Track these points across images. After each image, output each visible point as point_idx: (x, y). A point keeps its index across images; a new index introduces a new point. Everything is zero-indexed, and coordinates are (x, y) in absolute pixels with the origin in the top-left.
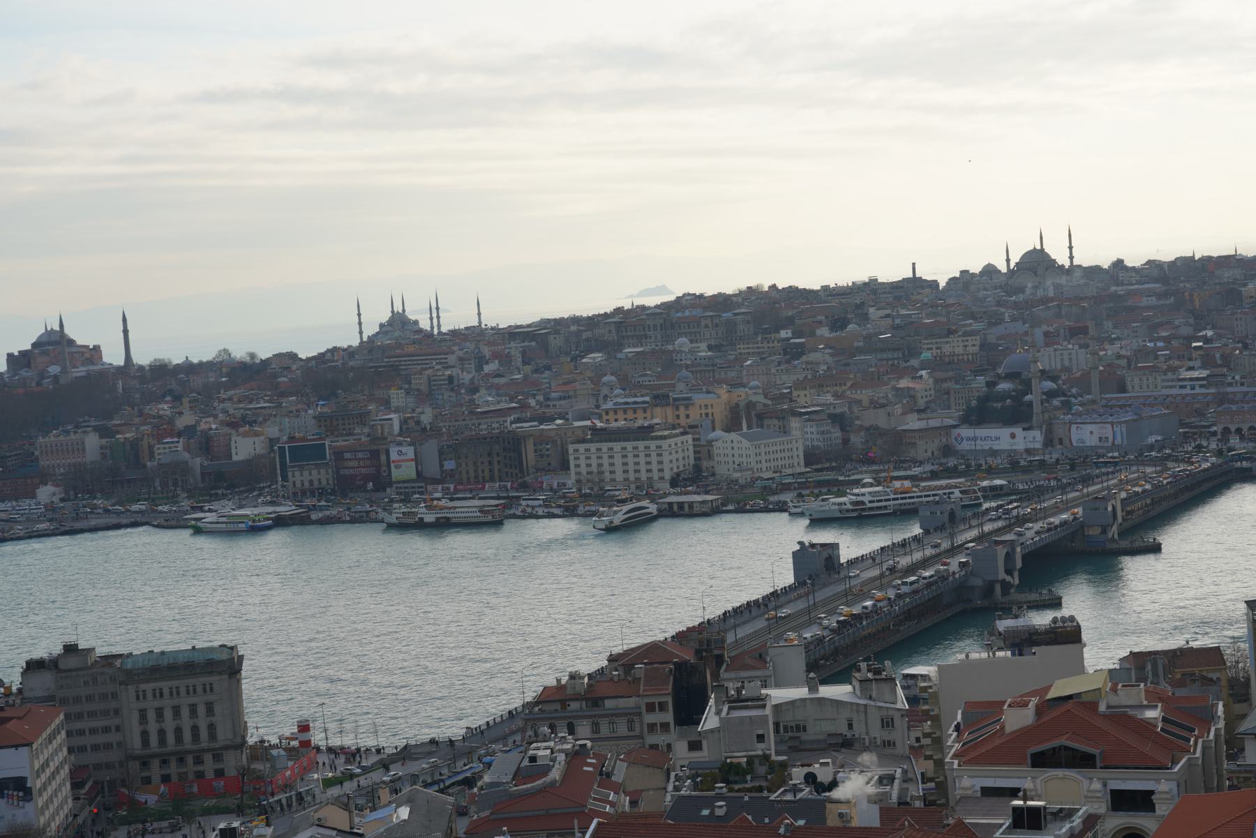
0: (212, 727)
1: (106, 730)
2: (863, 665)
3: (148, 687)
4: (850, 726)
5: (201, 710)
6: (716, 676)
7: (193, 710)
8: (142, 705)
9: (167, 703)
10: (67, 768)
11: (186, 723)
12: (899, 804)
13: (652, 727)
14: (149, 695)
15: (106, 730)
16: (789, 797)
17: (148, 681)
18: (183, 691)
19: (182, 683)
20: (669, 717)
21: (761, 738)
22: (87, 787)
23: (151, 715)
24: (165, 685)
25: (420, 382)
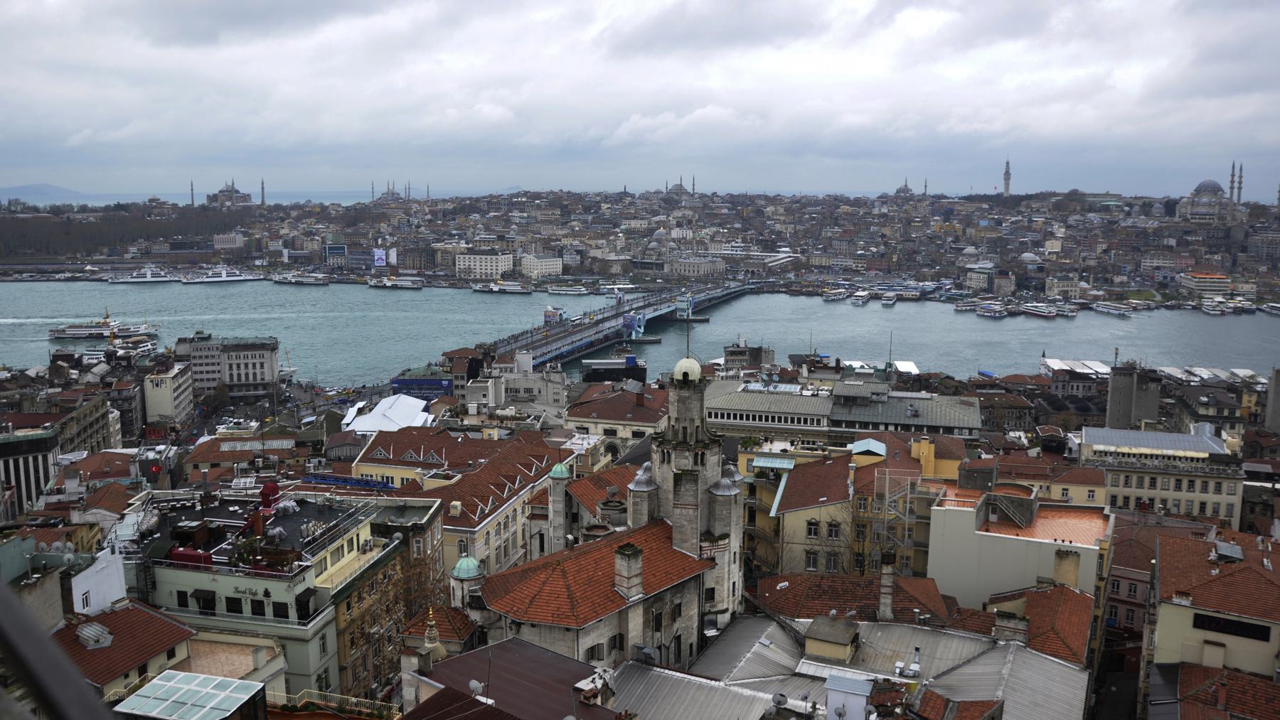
1: (214, 372)
3: (233, 354)
4: (540, 392)
5: (258, 366)
6: (489, 366)
7: (254, 365)
8: (230, 362)
9: (242, 361)
10: (191, 389)
11: (251, 371)
12: (542, 429)
13: (457, 387)
15: (214, 372)
17: (233, 351)
19: (249, 353)
21: (484, 396)
22: (202, 398)
23: (235, 367)
25: (395, 222)
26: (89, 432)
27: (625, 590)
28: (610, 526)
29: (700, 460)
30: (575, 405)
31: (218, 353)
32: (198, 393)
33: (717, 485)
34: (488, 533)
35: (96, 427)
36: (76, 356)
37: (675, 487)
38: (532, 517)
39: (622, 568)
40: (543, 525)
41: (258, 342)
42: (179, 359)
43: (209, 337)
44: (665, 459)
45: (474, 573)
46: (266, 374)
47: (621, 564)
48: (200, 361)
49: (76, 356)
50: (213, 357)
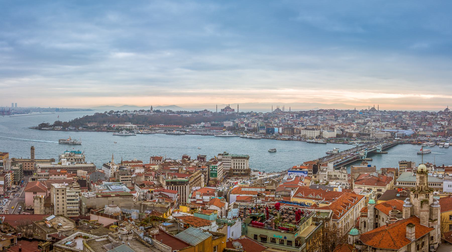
0: (244, 166)
2: (342, 167)
3: (235, 160)
5: (243, 164)
7: (241, 163)
8: (234, 162)
9: (238, 162)
11: (240, 165)
14: (235, 161)
16: (328, 186)
17: (235, 159)
18: (240, 161)
19: (240, 160)
20: (312, 172)
21: (325, 177)
23: (235, 164)
24: (238, 160)
26: (196, 181)
27: (410, 238)
28: (396, 218)
29: (427, 196)
30: (357, 181)
31: (230, 159)
32: (224, 171)
33: (433, 204)
34: (342, 221)
35: (198, 179)
36: (189, 157)
37: (421, 204)
38: (362, 216)
39: (409, 231)
40: (365, 219)
41: (243, 156)
42: (220, 160)
43: (228, 154)
44: (416, 196)
45: (357, 233)
46: (245, 167)
47: (408, 230)
48: (225, 161)
49: (189, 157)
50: (229, 160)
